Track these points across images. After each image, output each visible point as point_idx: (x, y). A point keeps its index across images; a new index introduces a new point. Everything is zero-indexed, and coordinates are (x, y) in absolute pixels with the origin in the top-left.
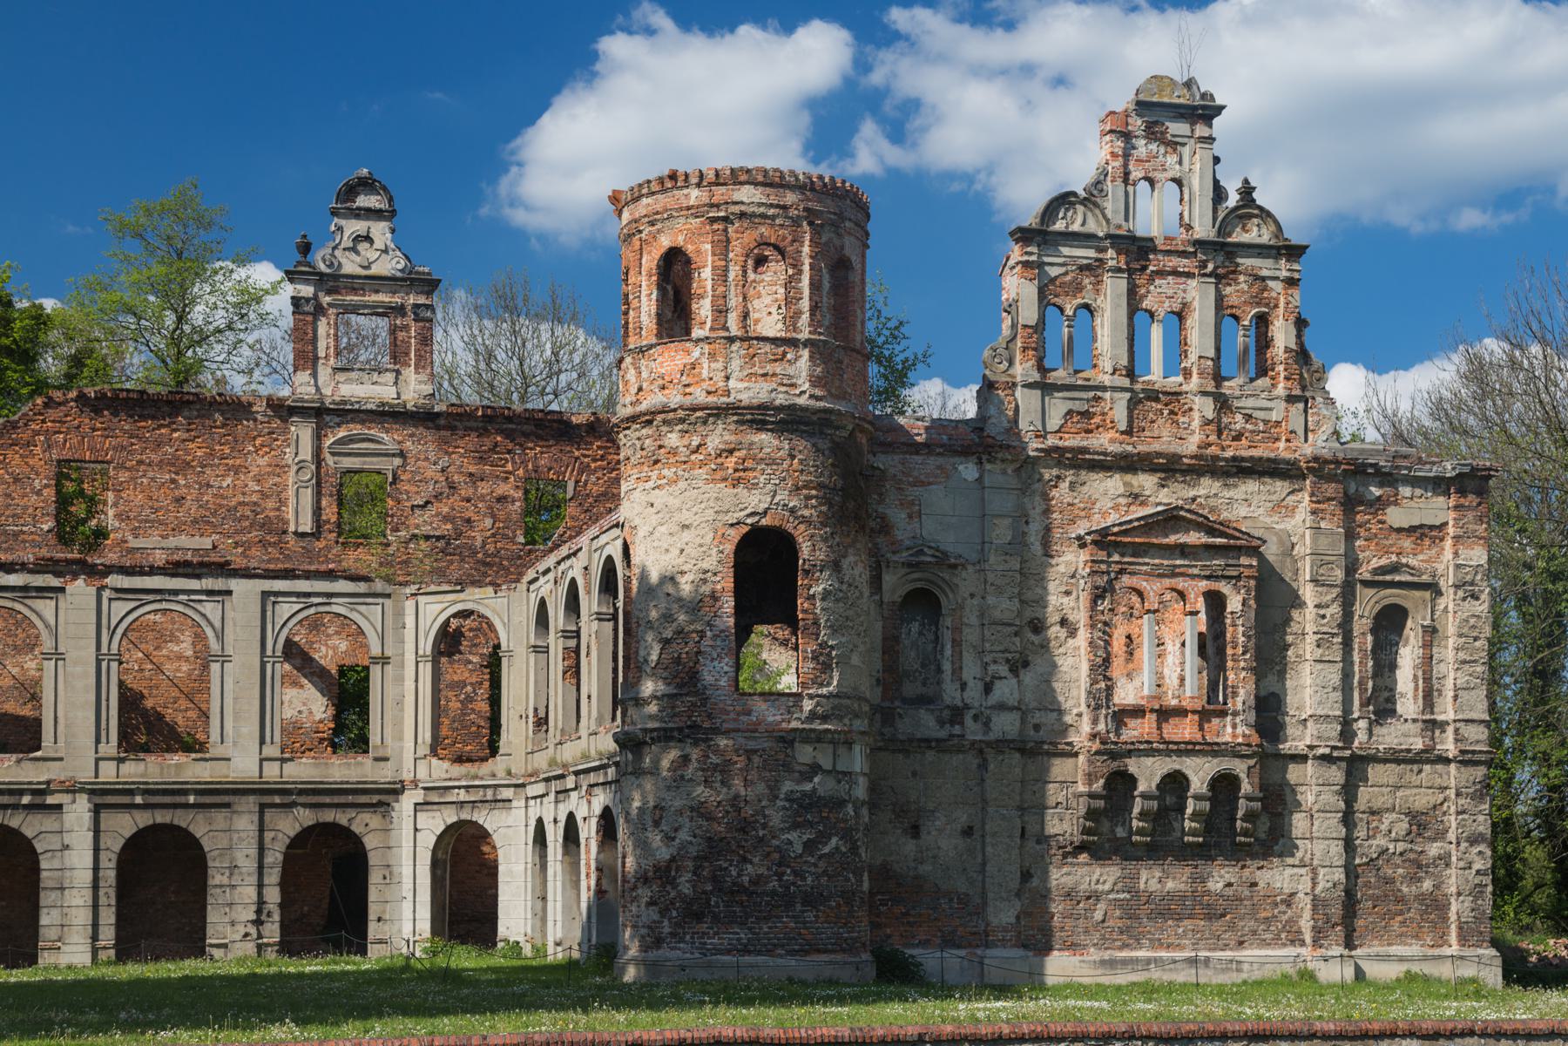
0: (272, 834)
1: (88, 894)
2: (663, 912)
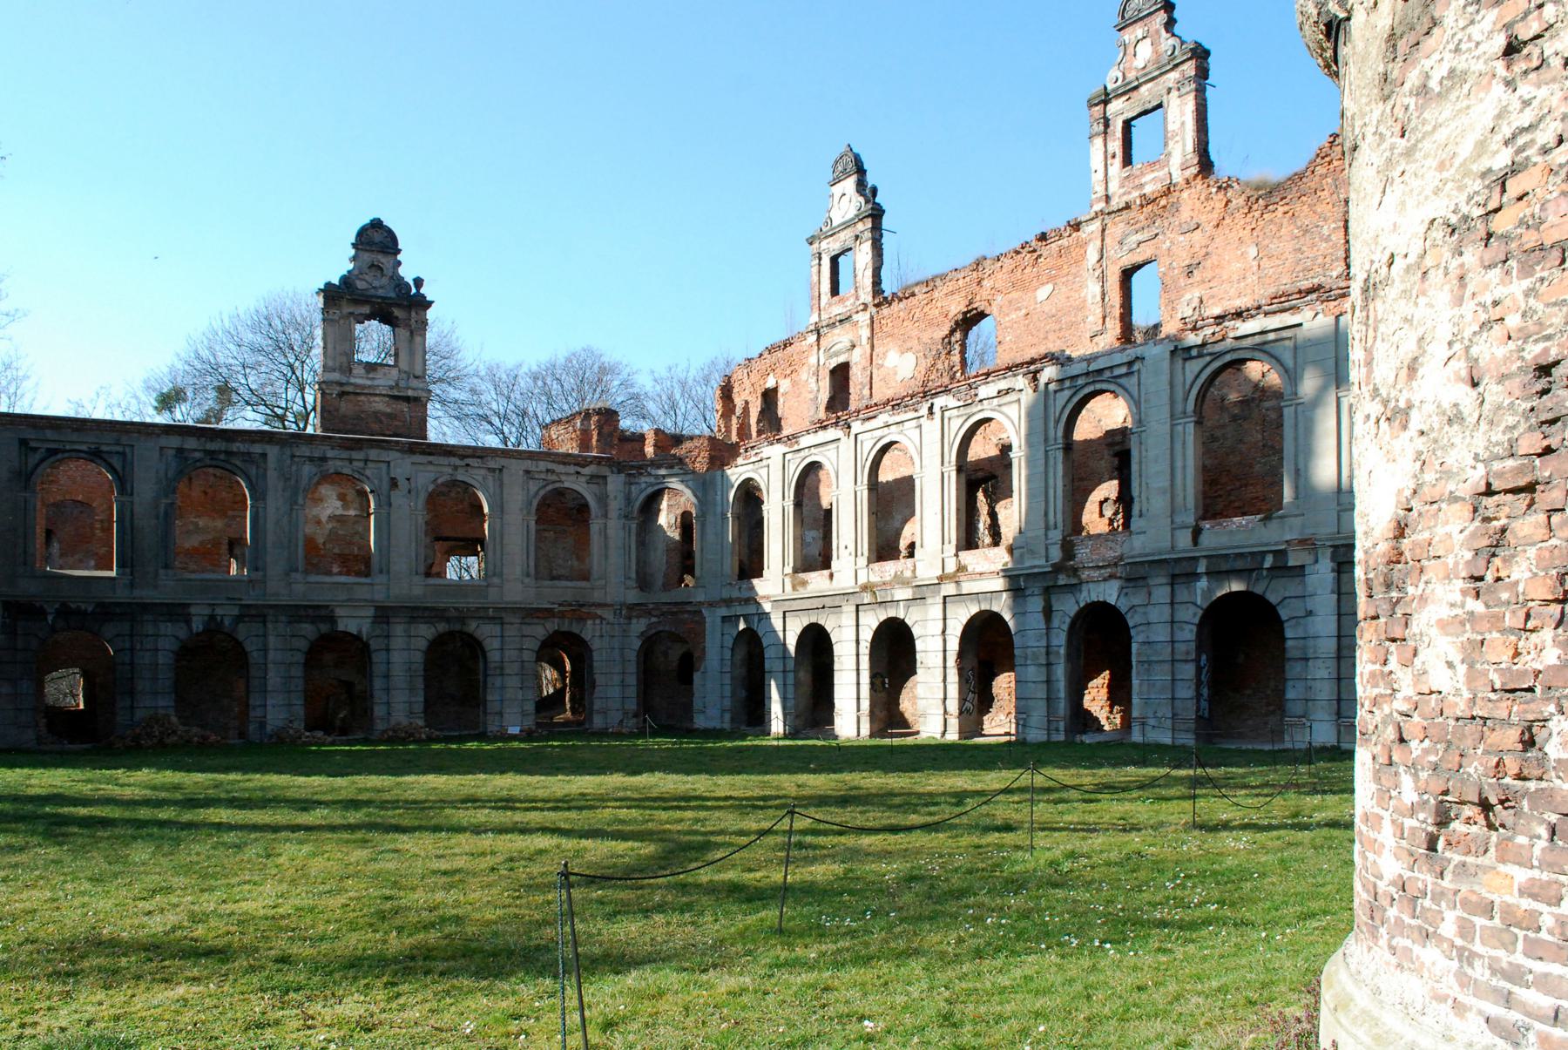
1: (1332, 664)
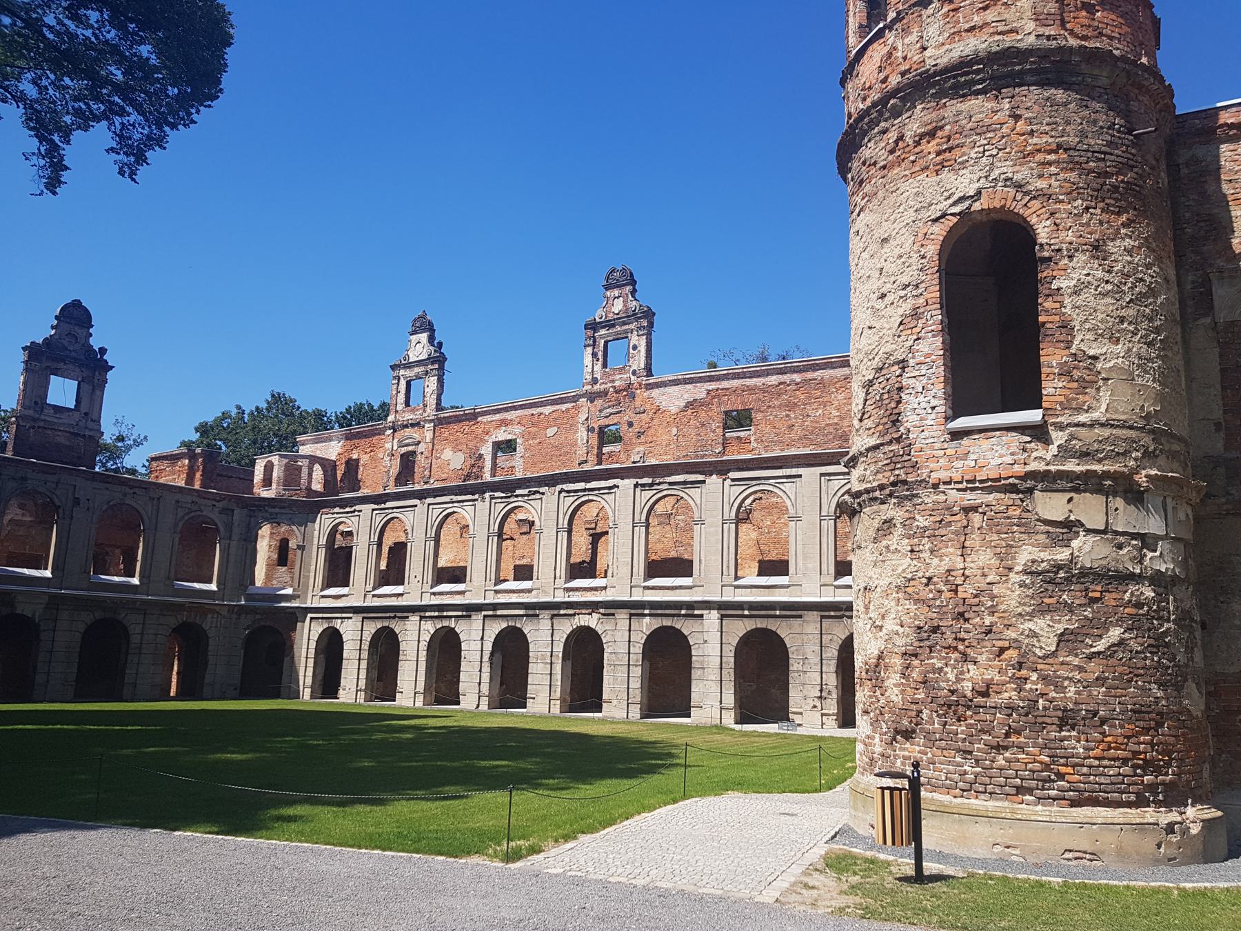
0: (830, 637)
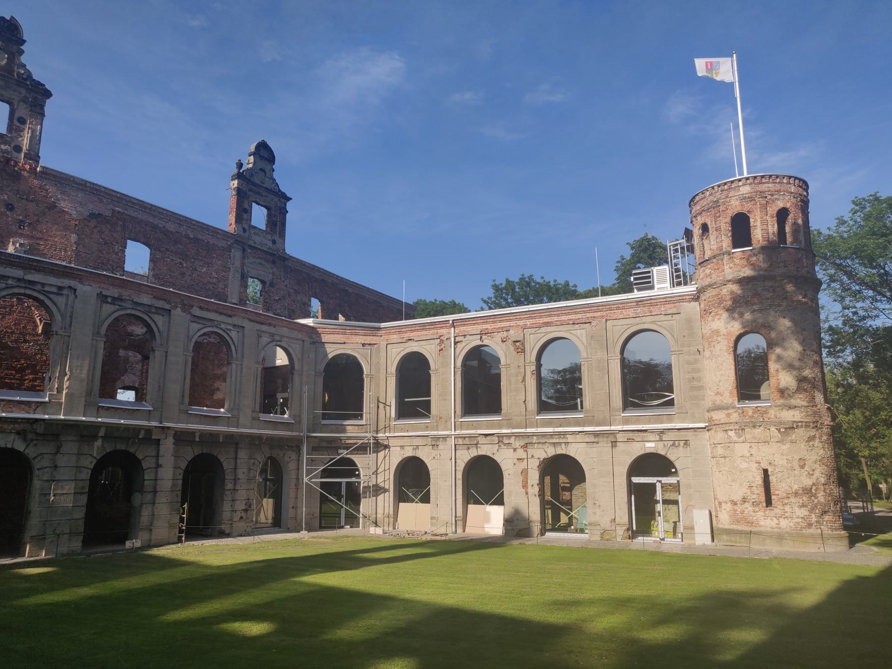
2: (811, 511)
